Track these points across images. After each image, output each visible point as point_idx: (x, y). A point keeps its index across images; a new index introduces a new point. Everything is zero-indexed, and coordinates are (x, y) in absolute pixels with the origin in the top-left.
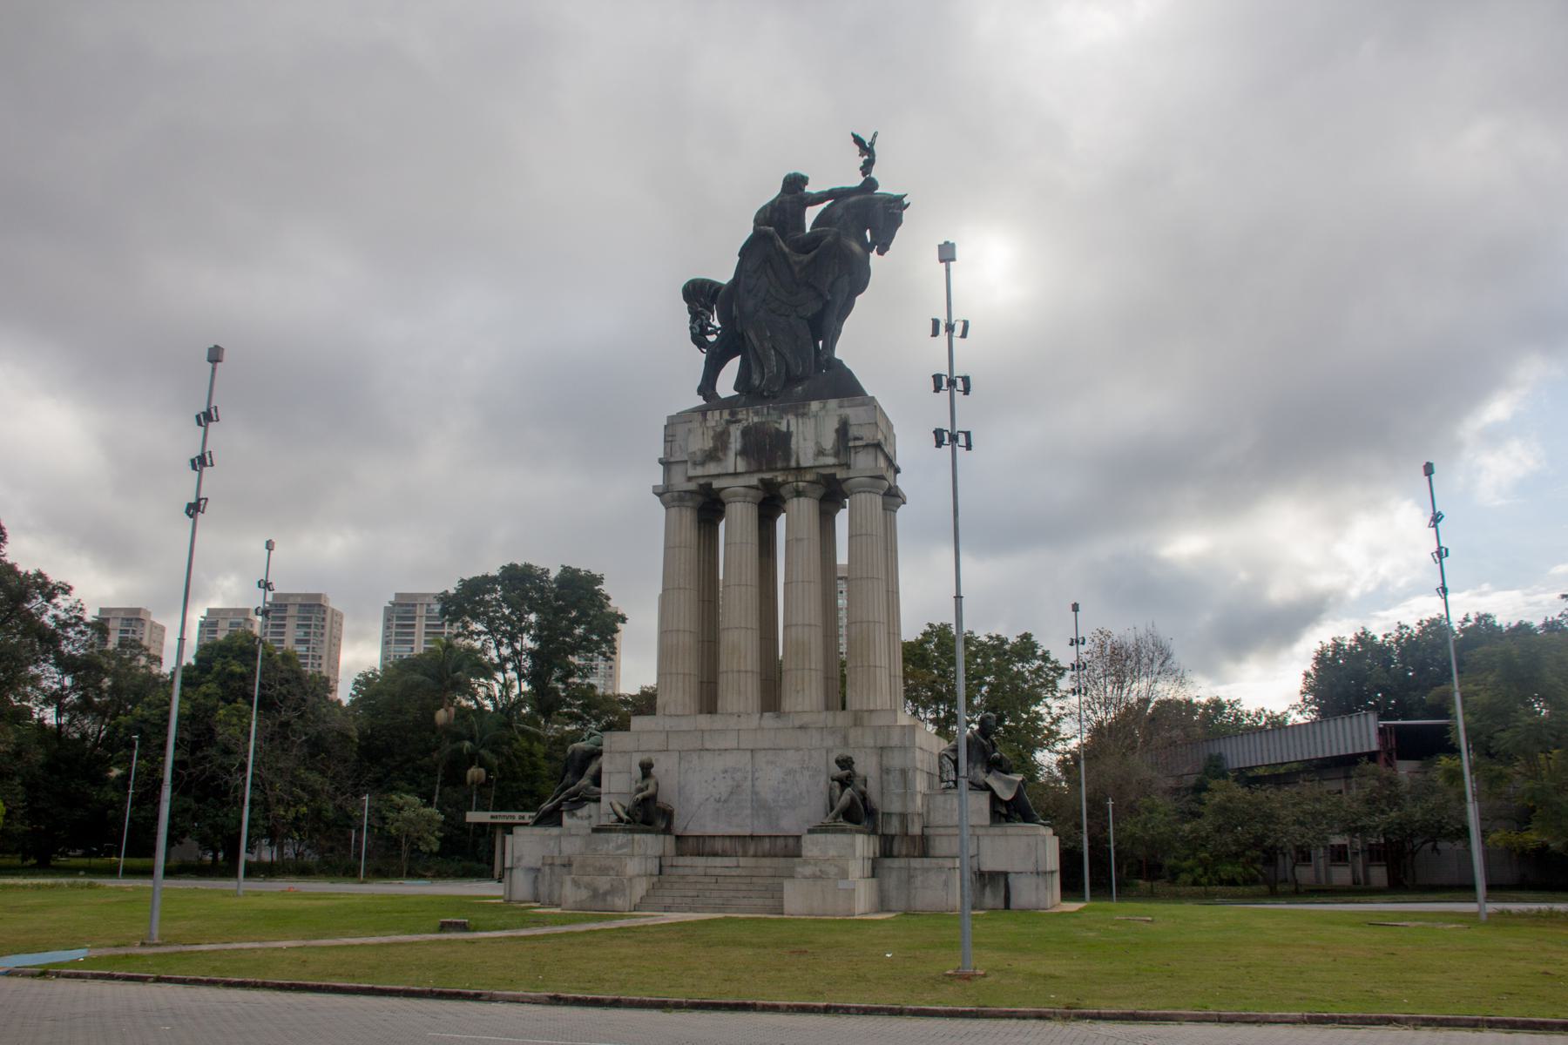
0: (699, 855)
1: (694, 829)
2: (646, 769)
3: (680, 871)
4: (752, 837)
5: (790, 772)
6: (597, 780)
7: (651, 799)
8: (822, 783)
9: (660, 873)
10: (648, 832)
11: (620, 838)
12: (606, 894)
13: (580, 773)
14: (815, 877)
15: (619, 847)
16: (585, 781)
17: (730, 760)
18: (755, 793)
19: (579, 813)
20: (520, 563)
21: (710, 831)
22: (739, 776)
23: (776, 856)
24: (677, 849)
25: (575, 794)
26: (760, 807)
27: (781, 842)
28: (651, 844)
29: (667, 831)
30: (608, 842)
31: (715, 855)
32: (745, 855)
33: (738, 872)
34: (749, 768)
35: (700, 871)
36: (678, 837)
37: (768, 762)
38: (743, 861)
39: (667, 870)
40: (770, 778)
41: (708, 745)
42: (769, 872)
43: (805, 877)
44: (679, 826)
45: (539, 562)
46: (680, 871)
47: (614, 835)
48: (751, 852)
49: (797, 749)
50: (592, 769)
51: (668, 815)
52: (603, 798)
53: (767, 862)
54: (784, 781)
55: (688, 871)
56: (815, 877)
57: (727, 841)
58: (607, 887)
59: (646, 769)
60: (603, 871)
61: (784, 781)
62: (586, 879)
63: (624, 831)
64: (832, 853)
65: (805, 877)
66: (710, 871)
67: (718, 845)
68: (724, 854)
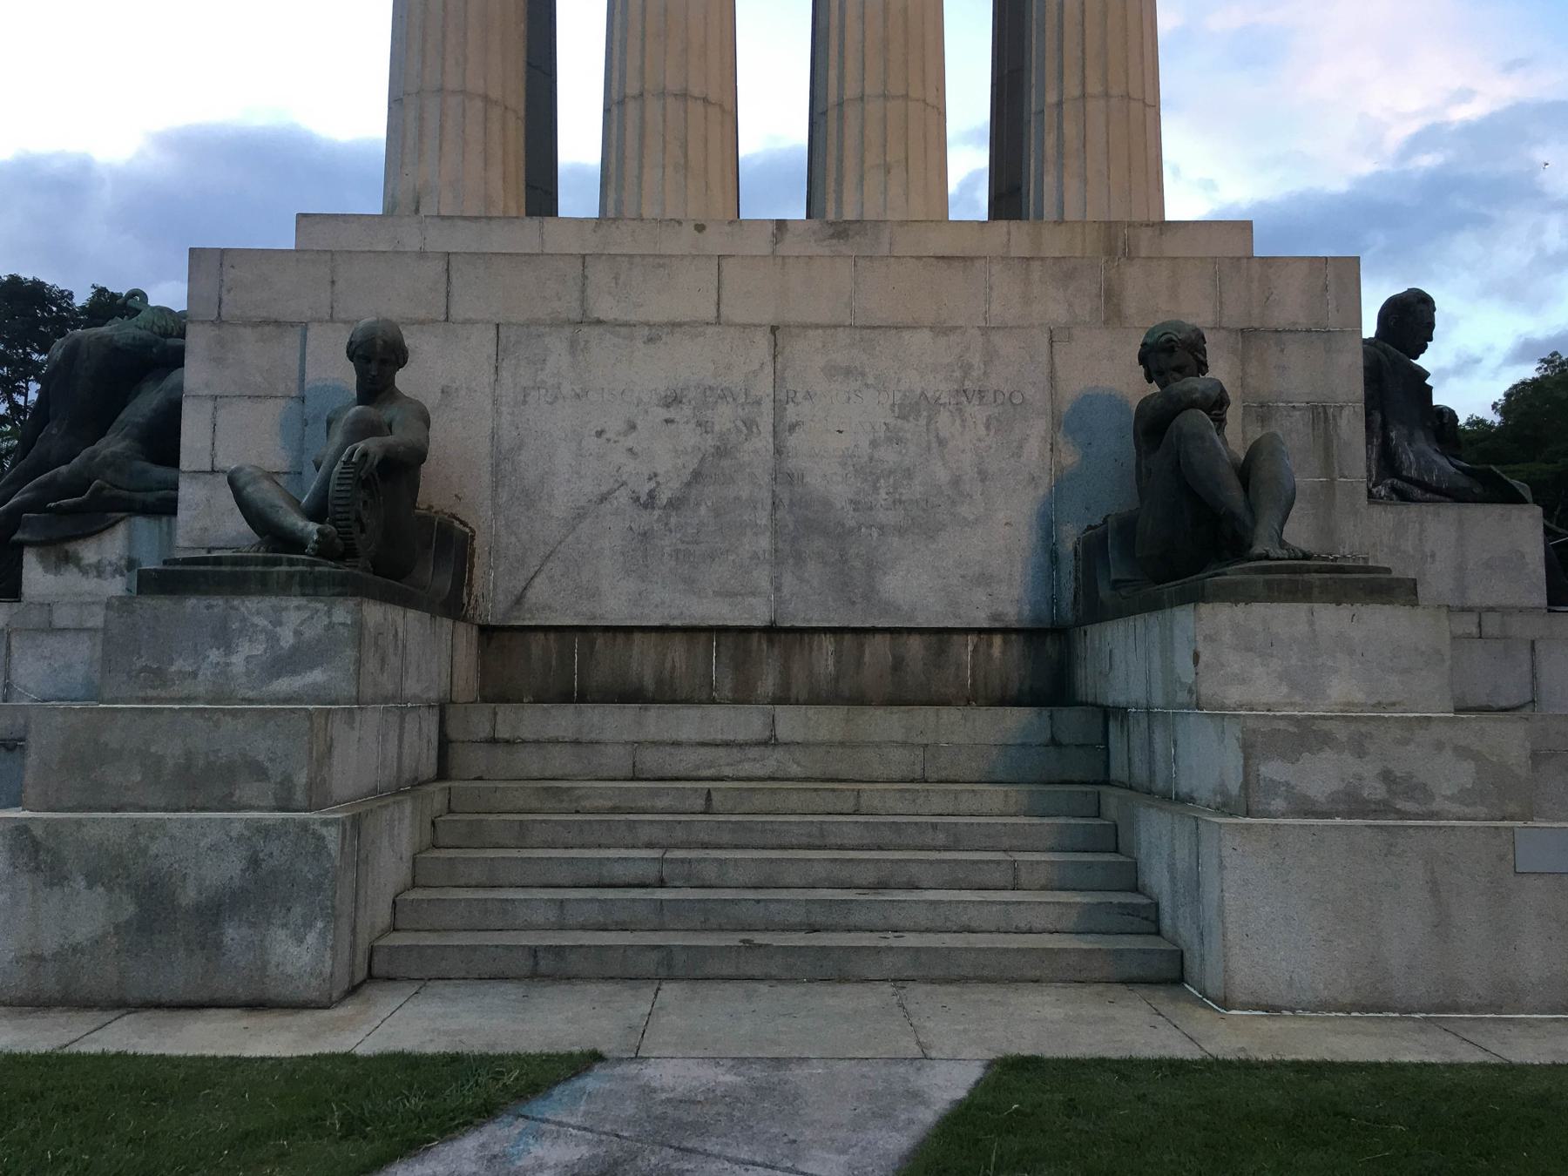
0: (566, 697)
1: (554, 604)
2: (378, 358)
3: (531, 762)
4: (772, 631)
5: (908, 408)
6: (162, 440)
7: (398, 470)
8: (1035, 448)
9: (442, 774)
10: (406, 601)
11: (294, 618)
12: (214, 911)
13: (98, 421)
14: (1353, 804)
15: (282, 664)
16: (112, 445)
17: (689, 361)
18: (784, 477)
19: (89, 552)
20: (27, 274)
21: (615, 609)
22: (724, 416)
23: (859, 700)
24: (484, 671)
25: (76, 486)
26: (802, 524)
27: (877, 650)
28: (424, 651)
29: (453, 606)
30: (224, 638)
31: (630, 695)
32: (743, 696)
33: (772, 761)
34: (764, 386)
35: (614, 758)
36: (487, 631)
37: (831, 371)
38: (792, 722)
39: (471, 759)
40: (838, 432)
41: (605, 307)
42: (900, 761)
43: (1306, 808)
44: (492, 589)
45: (53, 279)
46: (531, 762)
47: (253, 608)
48: (768, 683)
49: (941, 329)
50: (145, 403)
51: (452, 544)
52: (189, 492)
53: (886, 723)
54: (895, 439)
55: (560, 760)
56: (1353, 804)
57: (678, 653)
58: (227, 870)
59: (378, 358)
60: (202, 784)
61: (895, 439)
62: (104, 825)
63: (311, 586)
64: (1342, 689)
65: (1306, 808)
66: (651, 760)
67: (642, 661)
68: (665, 694)
